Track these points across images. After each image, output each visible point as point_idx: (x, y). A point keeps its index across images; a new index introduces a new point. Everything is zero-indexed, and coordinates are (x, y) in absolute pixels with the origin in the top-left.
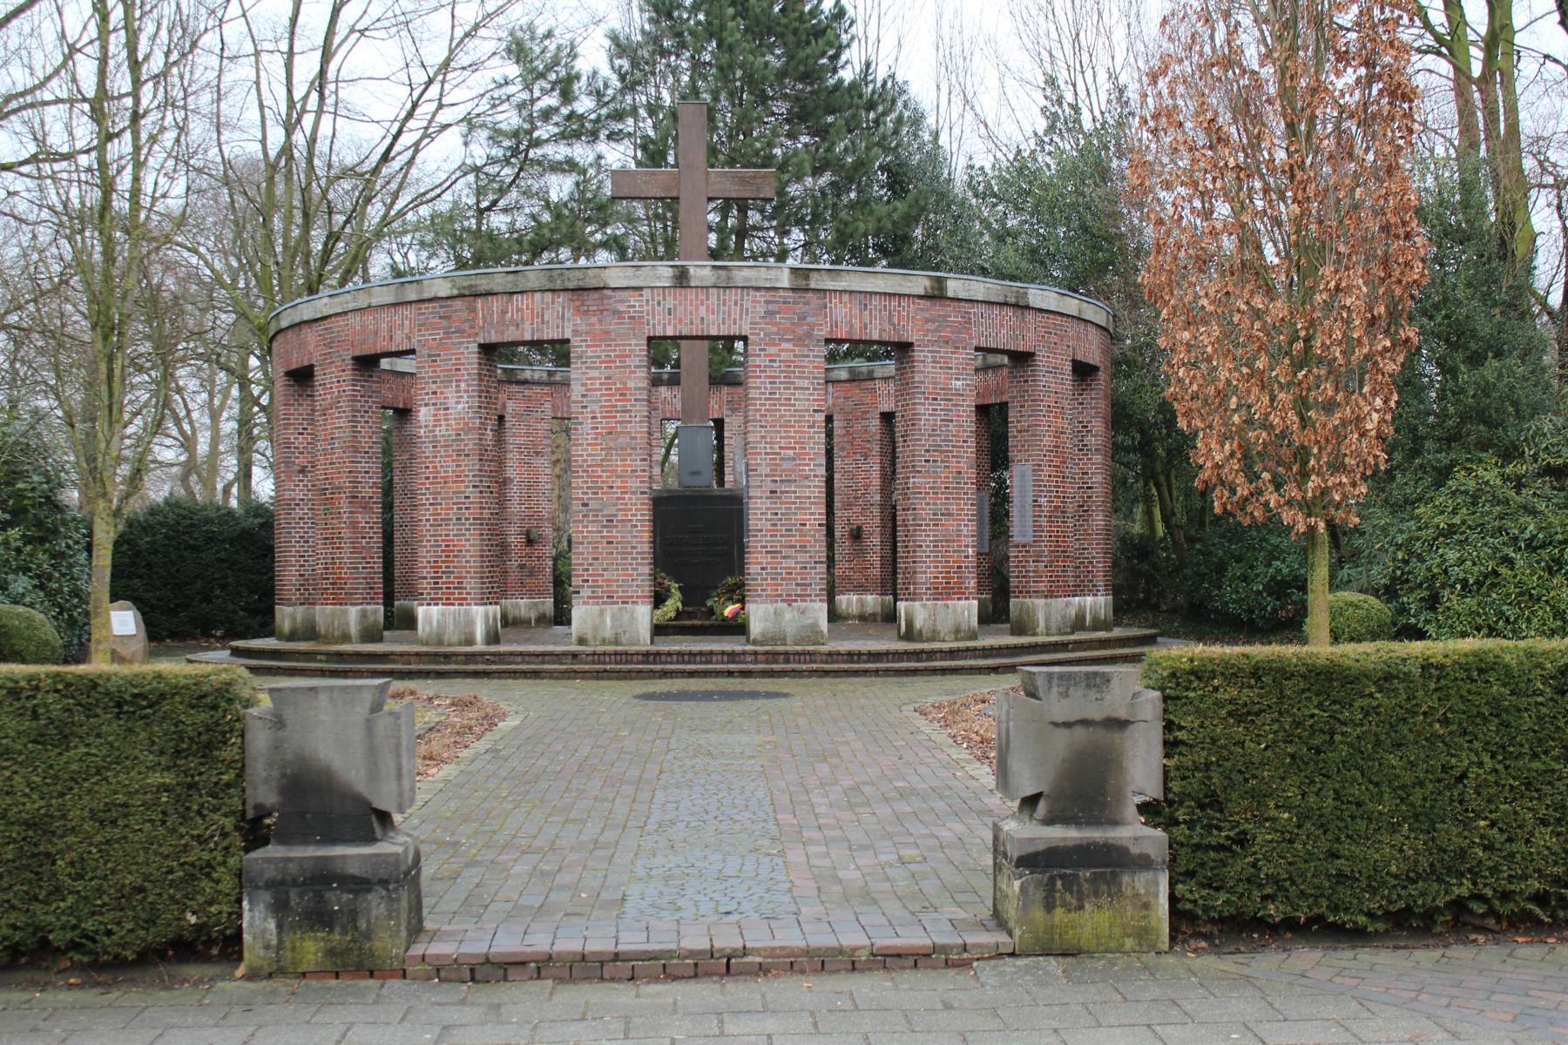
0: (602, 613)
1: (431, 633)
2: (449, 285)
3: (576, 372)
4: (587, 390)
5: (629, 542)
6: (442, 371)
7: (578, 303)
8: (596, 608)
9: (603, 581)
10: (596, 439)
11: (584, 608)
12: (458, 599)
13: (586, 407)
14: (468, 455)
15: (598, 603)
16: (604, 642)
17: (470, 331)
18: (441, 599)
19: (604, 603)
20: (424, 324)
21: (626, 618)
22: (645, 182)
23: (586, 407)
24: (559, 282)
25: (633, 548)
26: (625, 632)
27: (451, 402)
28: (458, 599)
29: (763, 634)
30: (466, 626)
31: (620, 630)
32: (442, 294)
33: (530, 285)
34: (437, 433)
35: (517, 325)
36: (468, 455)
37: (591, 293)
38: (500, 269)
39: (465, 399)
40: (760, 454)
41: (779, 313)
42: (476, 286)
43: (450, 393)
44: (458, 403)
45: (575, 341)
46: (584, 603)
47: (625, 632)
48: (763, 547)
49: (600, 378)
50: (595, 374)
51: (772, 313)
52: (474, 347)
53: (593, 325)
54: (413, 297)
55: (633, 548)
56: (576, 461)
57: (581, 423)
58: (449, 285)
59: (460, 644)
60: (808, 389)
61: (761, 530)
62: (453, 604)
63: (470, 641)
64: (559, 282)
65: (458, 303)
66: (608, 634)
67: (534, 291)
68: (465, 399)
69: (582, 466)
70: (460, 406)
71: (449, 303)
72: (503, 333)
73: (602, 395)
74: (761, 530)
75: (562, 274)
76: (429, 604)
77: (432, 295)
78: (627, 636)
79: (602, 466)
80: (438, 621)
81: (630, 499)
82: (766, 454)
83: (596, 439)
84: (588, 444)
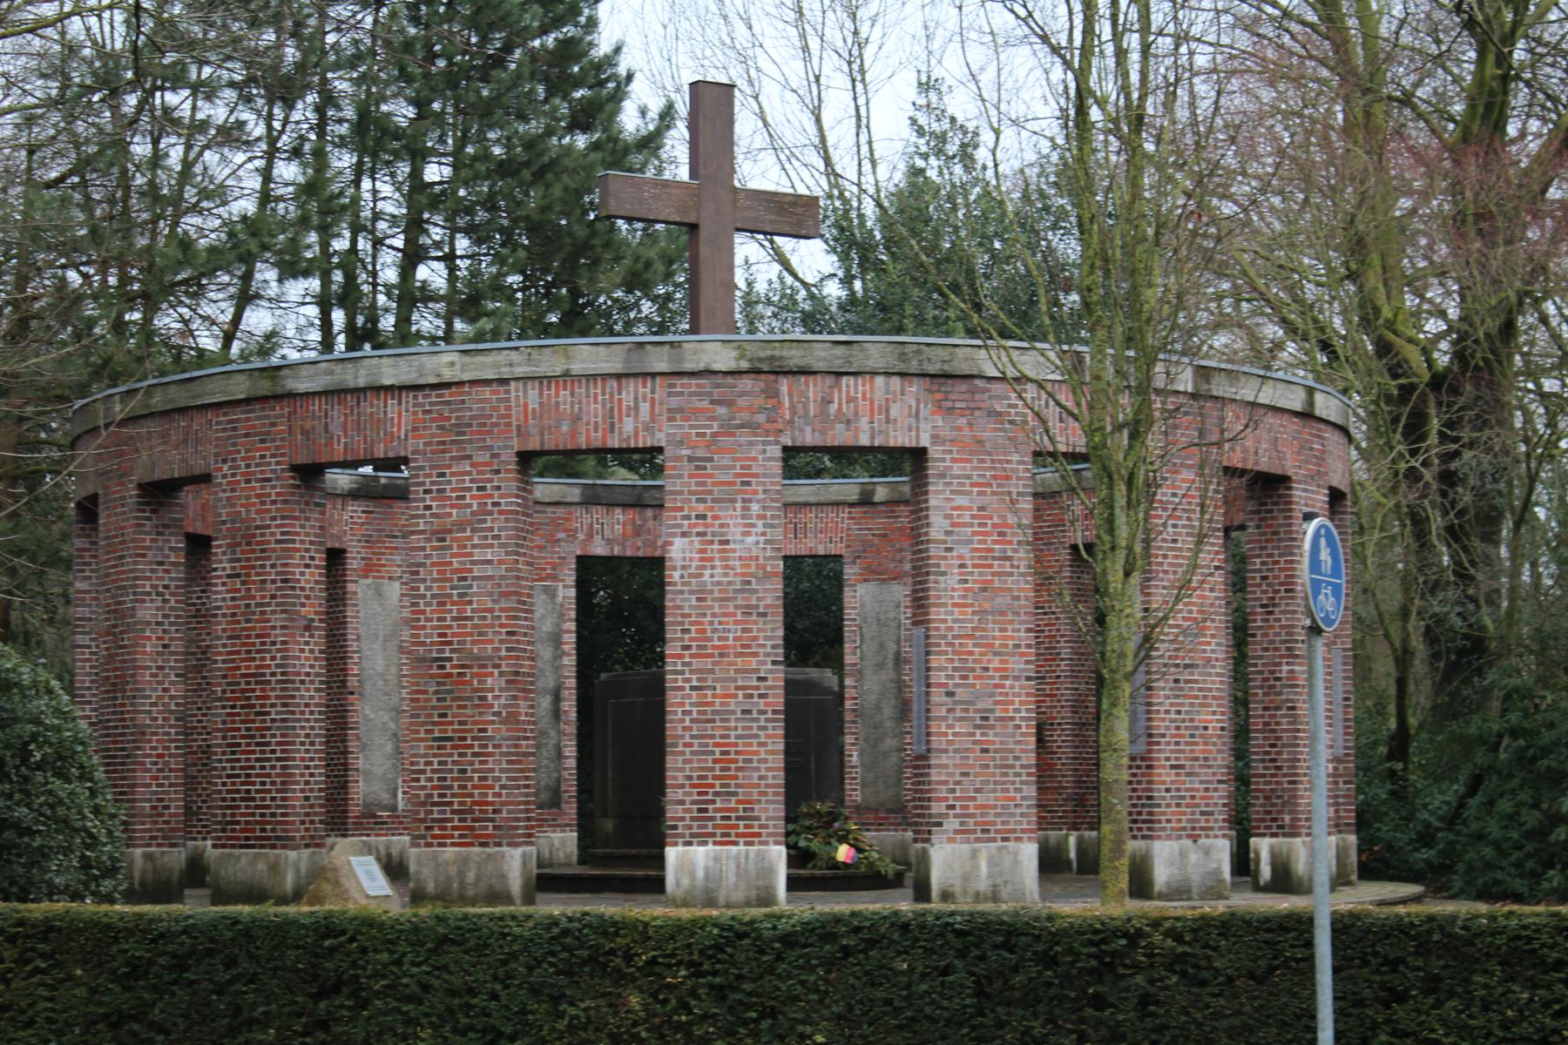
0: (974, 855)
1: (693, 887)
2: (734, 354)
3: (937, 498)
4: (954, 525)
5: (1011, 751)
7: (938, 396)
8: (967, 847)
9: (977, 807)
10: (964, 597)
11: (949, 847)
12: (744, 835)
13: (949, 550)
14: (764, 615)
15: (968, 841)
16: (978, 897)
17: (768, 426)
18: (714, 835)
19: (978, 840)
20: (680, 410)
21: (1007, 861)
22: (655, 198)
23: (949, 550)
24: (914, 363)
25: (1017, 758)
26: (1006, 882)
27: (735, 532)
28: (744, 835)
29: (1168, 884)
30: (758, 877)
31: (999, 881)
33: (871, 364)
34: (706, 578)
35: (848, 422)
36: (764, 615)
37: (958, 381)
38: (825, 337)
39: (760, 529)
42: (781, 358)
45: (934, 452)
46: (951, 840)
47: (1006, 882)
49: (970, 509)
50: (961, 501)
52: (776, 451)
53: (960, 429)
54: (663, 366)
55: (1017, 758)
56: (937, 629)
57: (944, 574)
58: (734, 354)
59: (748, 904)
62: (735, 843)
63: (767, 899)
64: (914, 363)
65: (747, 383)
66: (983, 885)
67: (874, 373)
68: (760, 529)
69: (945, 637)
70: (750, 540)
71: (730, 380)
72: (823, 432)
73: (975, 533)
75: (918, 352)
76: (689, 844)
77: (701, 366)
78: (1009, 888)
79: (971, 637)
80: (707, 869)
81: (1012, 687)
83: (964, 597)
84: (955, 605)
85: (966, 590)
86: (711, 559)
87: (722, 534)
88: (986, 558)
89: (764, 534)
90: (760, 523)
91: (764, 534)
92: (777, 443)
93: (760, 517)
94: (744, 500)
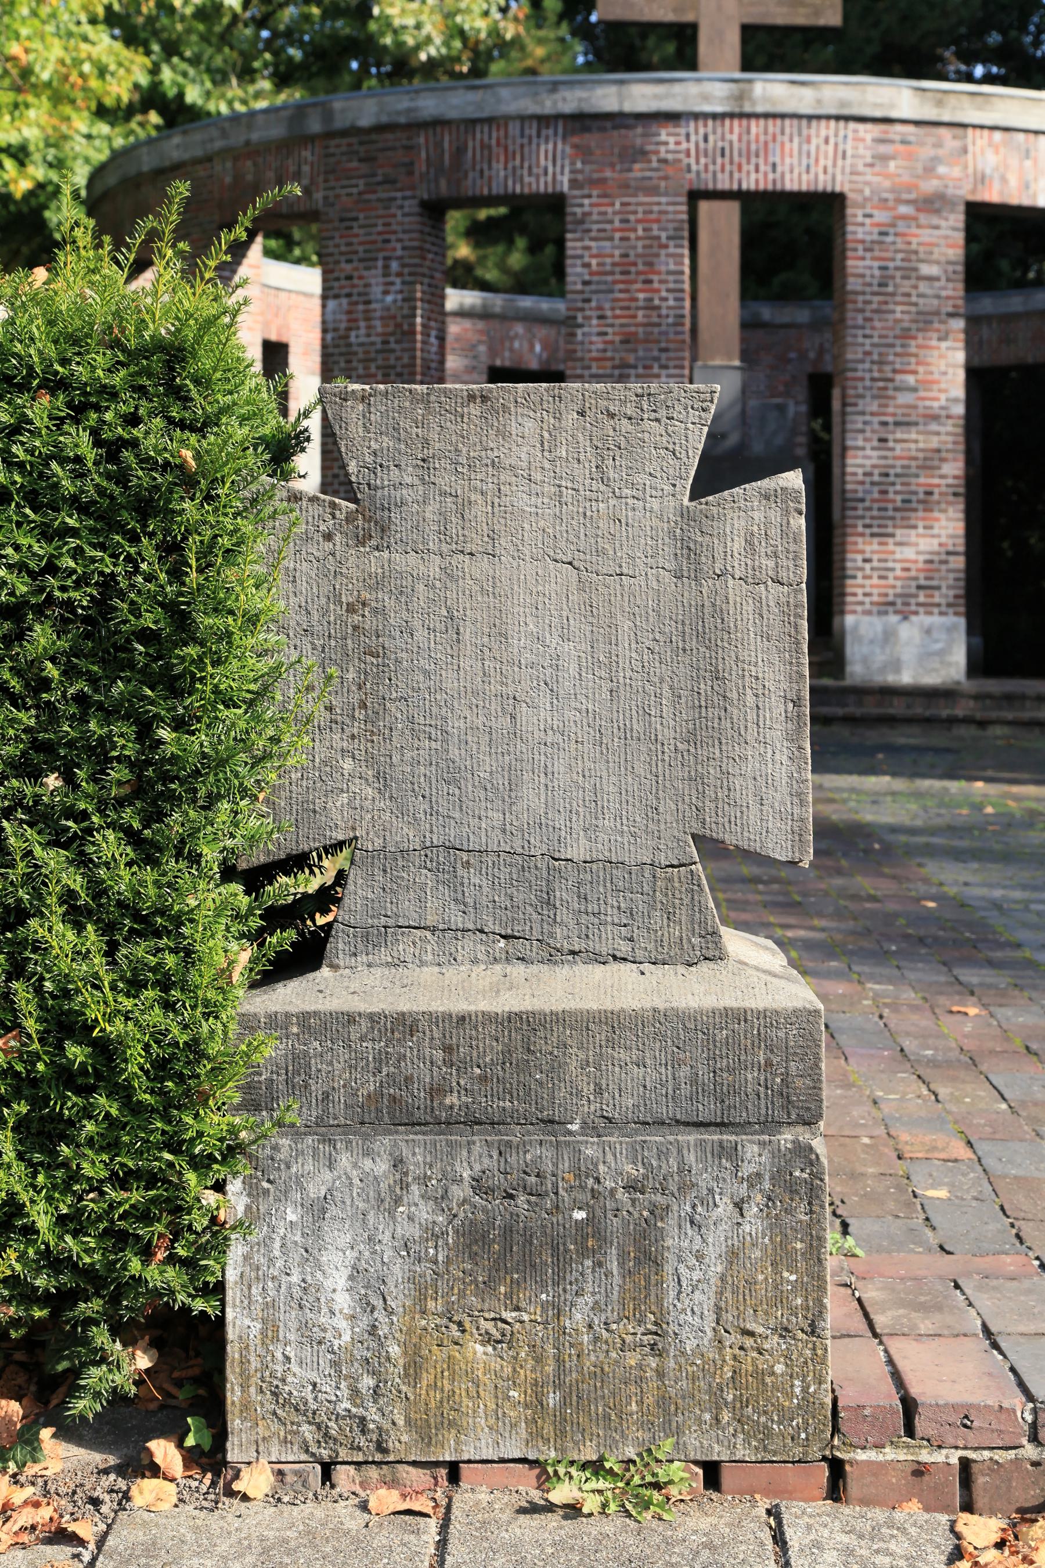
6: (361, 243)
27: (376, 291)
32: (365, 122)
34: (353, 339)
40: (862, 379)
41: (893, 158)
43: (375, 280)
44: (386, 293)
48: (865, 526)
51: (884, 158)
52: (411, 206)
60: (938, 279)
61: (862, 500)
70: (389, 299)
71: (374, 137)
74: (862, 500)
82: (873, 379)
83: (605, 351)
85: (606, 342)
86: (356, 320)
87: (366, 294)
88: (628, 308)
89: (401, 292)
90: (398, 280)
91: (401, 292)
92: (414, 197)
93: (399, 274)
94: (386, 259)
